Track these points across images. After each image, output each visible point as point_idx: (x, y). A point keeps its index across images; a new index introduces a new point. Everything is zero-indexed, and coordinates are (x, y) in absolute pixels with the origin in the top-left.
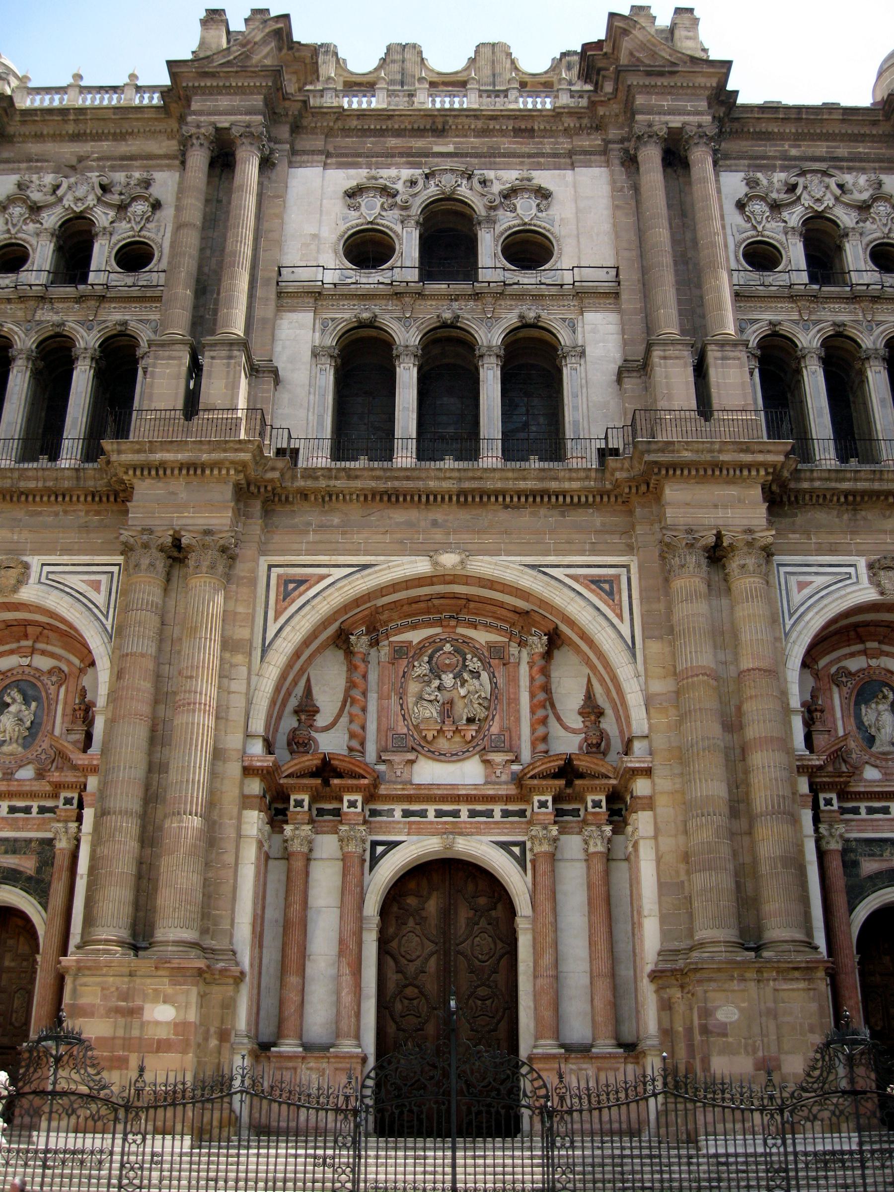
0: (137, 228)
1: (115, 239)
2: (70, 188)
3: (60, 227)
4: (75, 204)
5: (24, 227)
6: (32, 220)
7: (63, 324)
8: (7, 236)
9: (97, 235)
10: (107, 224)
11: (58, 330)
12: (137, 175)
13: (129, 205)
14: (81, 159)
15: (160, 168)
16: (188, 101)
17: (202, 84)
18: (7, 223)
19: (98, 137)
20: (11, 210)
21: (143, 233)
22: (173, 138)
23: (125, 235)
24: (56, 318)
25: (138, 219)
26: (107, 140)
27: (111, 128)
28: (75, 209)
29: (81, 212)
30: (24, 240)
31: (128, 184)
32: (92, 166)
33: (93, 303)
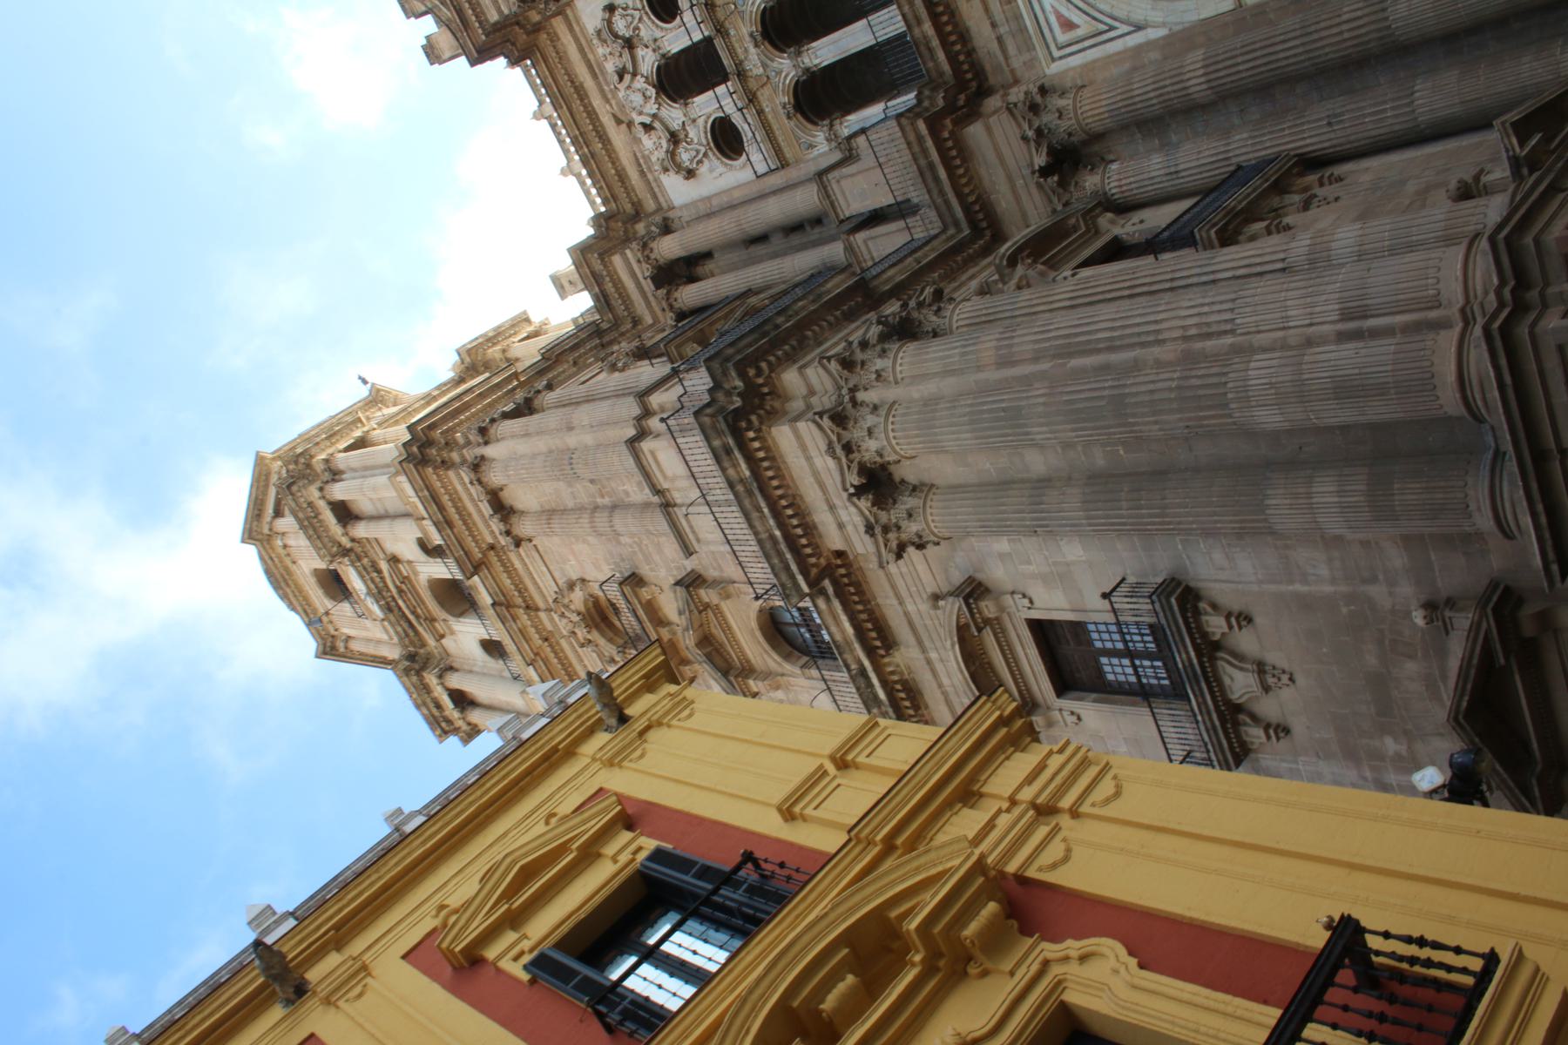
0: (637, 14)
1: (658, 34)
2: (641, 113)
3: (675, 102)
4: (650, 97)
5: (696, 141)
6: (686, 136)
7: (751, 35)
8: (710, 154)
9: (663, 56)
10: (650, 49)
11: (759, 38)
12: (601, 50)
13: (622, 38)
14: (619, 122)
15: (583, 30)
16: (498, 27)
17: (474, 18)
18: (700, 162)
19: (592, 115)
20: (687, 163)
21: (640, 6)
22: (555, 33)
23: (649, 23)
24: (752, 50)
25: (629, 19)
26: (590, 104)
27: (577, 105)
28: (654, 95)
29: (654, 86)
30: (706, 133)
31: (611, 54)
32: (617, 103)
33: (720, 14)
